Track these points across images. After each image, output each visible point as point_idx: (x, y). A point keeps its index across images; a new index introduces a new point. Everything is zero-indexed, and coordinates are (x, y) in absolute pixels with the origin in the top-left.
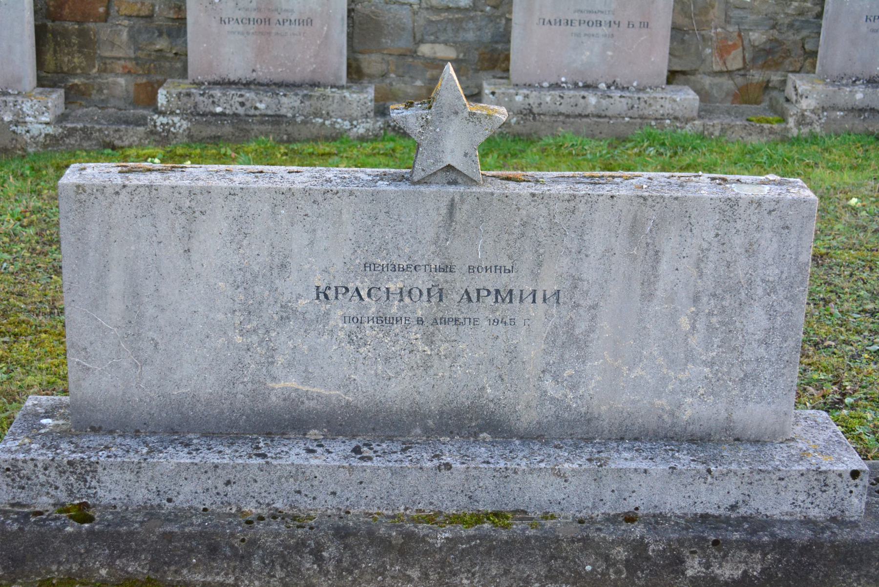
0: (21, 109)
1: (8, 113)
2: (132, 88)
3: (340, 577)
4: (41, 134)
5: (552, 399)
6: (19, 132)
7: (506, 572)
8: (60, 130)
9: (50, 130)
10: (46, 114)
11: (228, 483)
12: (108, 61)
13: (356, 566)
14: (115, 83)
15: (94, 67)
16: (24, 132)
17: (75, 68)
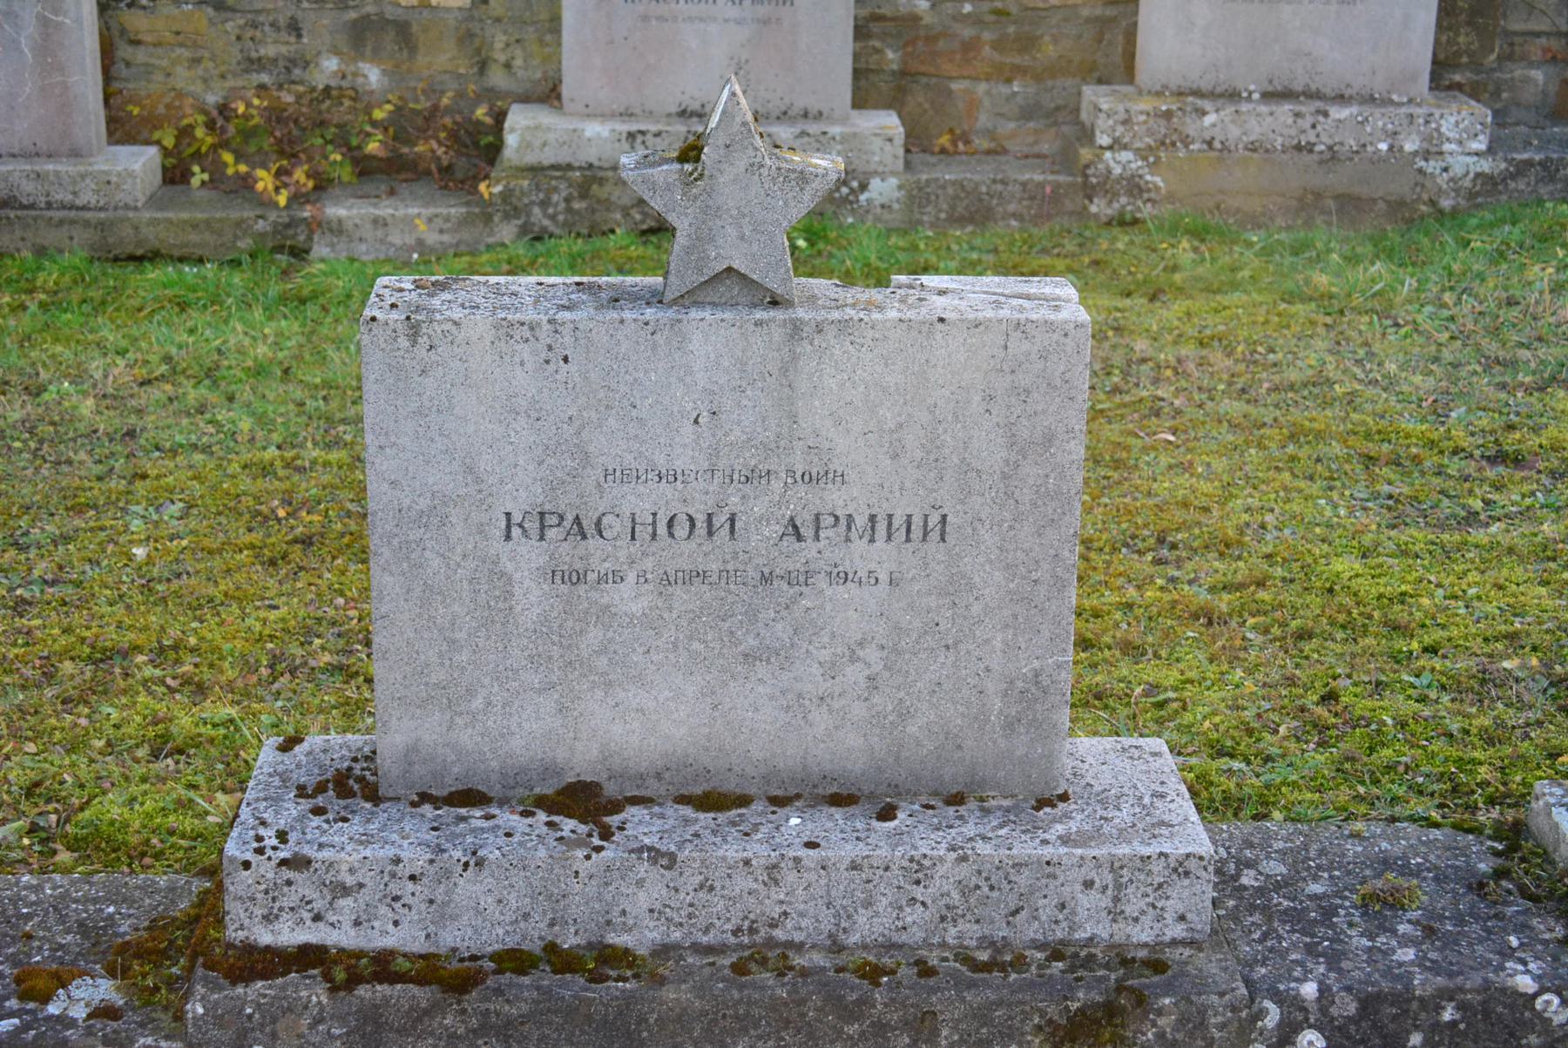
0: (1437, 130)
1: (1414, 136)
2: (1553, 89)
4: (1468, 173)
6: (1430, 170)
8: (1503, 166)
9: (1485, 166)
10: (1481, 137)
12: (1517, 40)
14: (1527, 80)
15: (1493, 50)
16: (1438, 171)
17: (1458, 54)
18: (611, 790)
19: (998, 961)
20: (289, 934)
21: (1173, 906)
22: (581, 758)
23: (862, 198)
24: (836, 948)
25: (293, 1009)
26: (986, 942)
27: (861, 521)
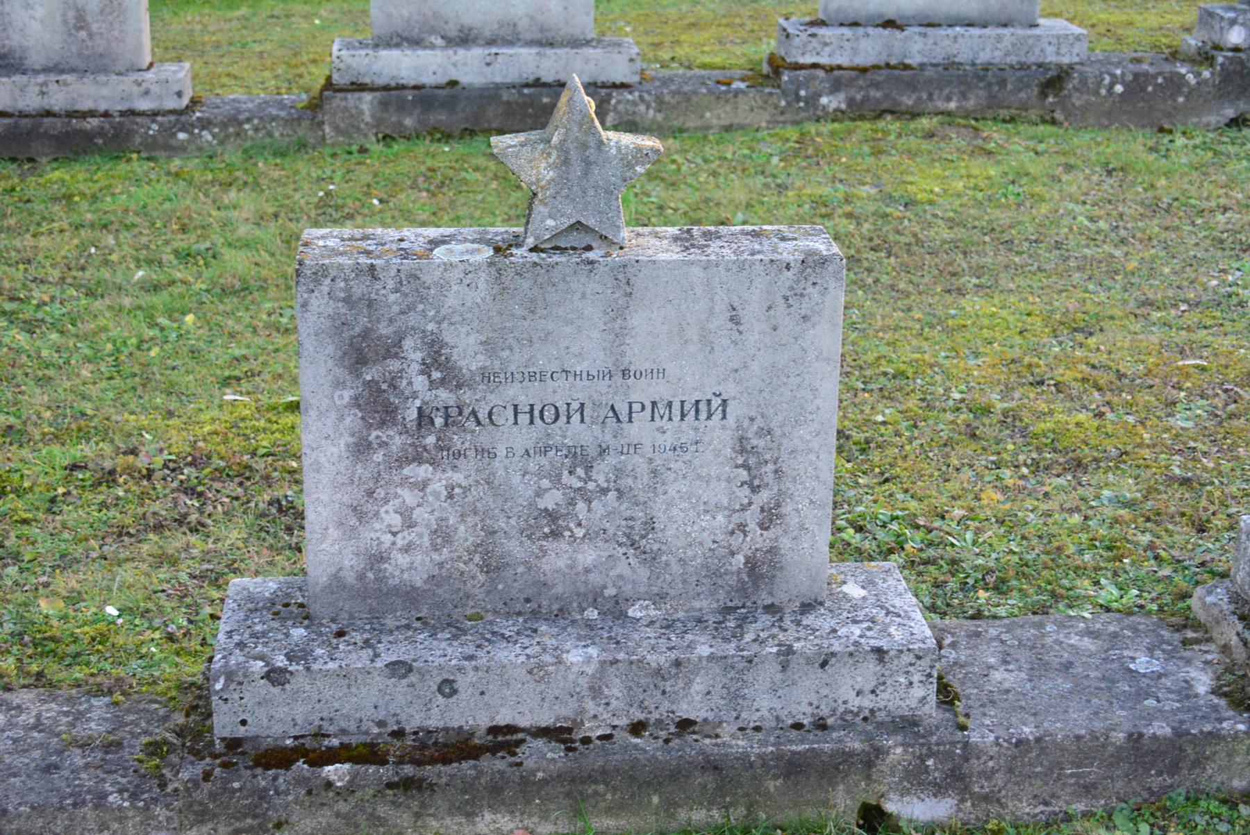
18: (899, 22)
19: (1023, 67)
20: (808, 60)
21: (1075, 51)
22: (890, 13)
24: (973, 64)
25: (814, 78)
26: (1019, 62)
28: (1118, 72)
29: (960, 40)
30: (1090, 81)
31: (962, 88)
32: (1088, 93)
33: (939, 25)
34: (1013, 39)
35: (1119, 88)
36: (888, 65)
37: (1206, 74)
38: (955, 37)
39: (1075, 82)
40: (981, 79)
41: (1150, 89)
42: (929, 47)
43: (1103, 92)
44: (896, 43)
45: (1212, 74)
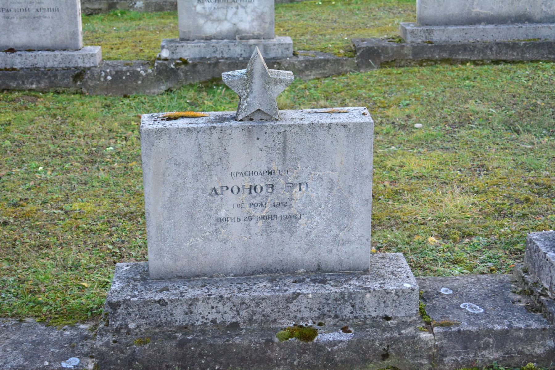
3: (497, 55)
5: (544, 12)
7: (538, 52)
11: (466, 34)
13: (500, 52)
18: (15, 49)
21: (91, 61)
22: (11, 45)
23: (135, 6)
24: (45, 68)
26: (66, 67)
27: (46, 9)
28: (108, 70)
29: (38, 57)
30: (95, 75)
31: (37, 79)
32: (95, 80)
33: (34, 50)
34: (62, 56)
35: (109, 78)
36: (6, 69)
37: (150, 71)
38: (35, 56)
39: (89, 75)
40: (46, 74)
41: (124, 78)
42: (24, 60)
43: (102, 79)
44: (8, 59)
45: (153, 71)
